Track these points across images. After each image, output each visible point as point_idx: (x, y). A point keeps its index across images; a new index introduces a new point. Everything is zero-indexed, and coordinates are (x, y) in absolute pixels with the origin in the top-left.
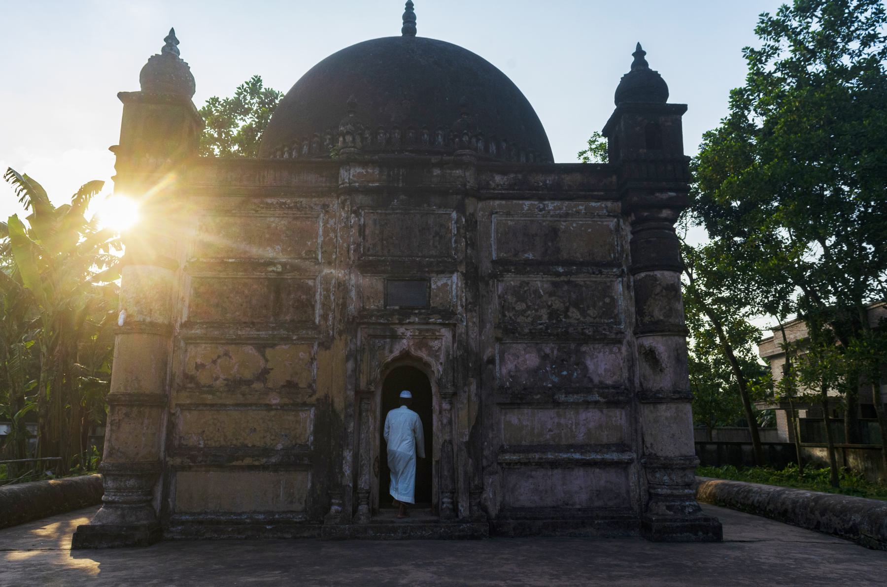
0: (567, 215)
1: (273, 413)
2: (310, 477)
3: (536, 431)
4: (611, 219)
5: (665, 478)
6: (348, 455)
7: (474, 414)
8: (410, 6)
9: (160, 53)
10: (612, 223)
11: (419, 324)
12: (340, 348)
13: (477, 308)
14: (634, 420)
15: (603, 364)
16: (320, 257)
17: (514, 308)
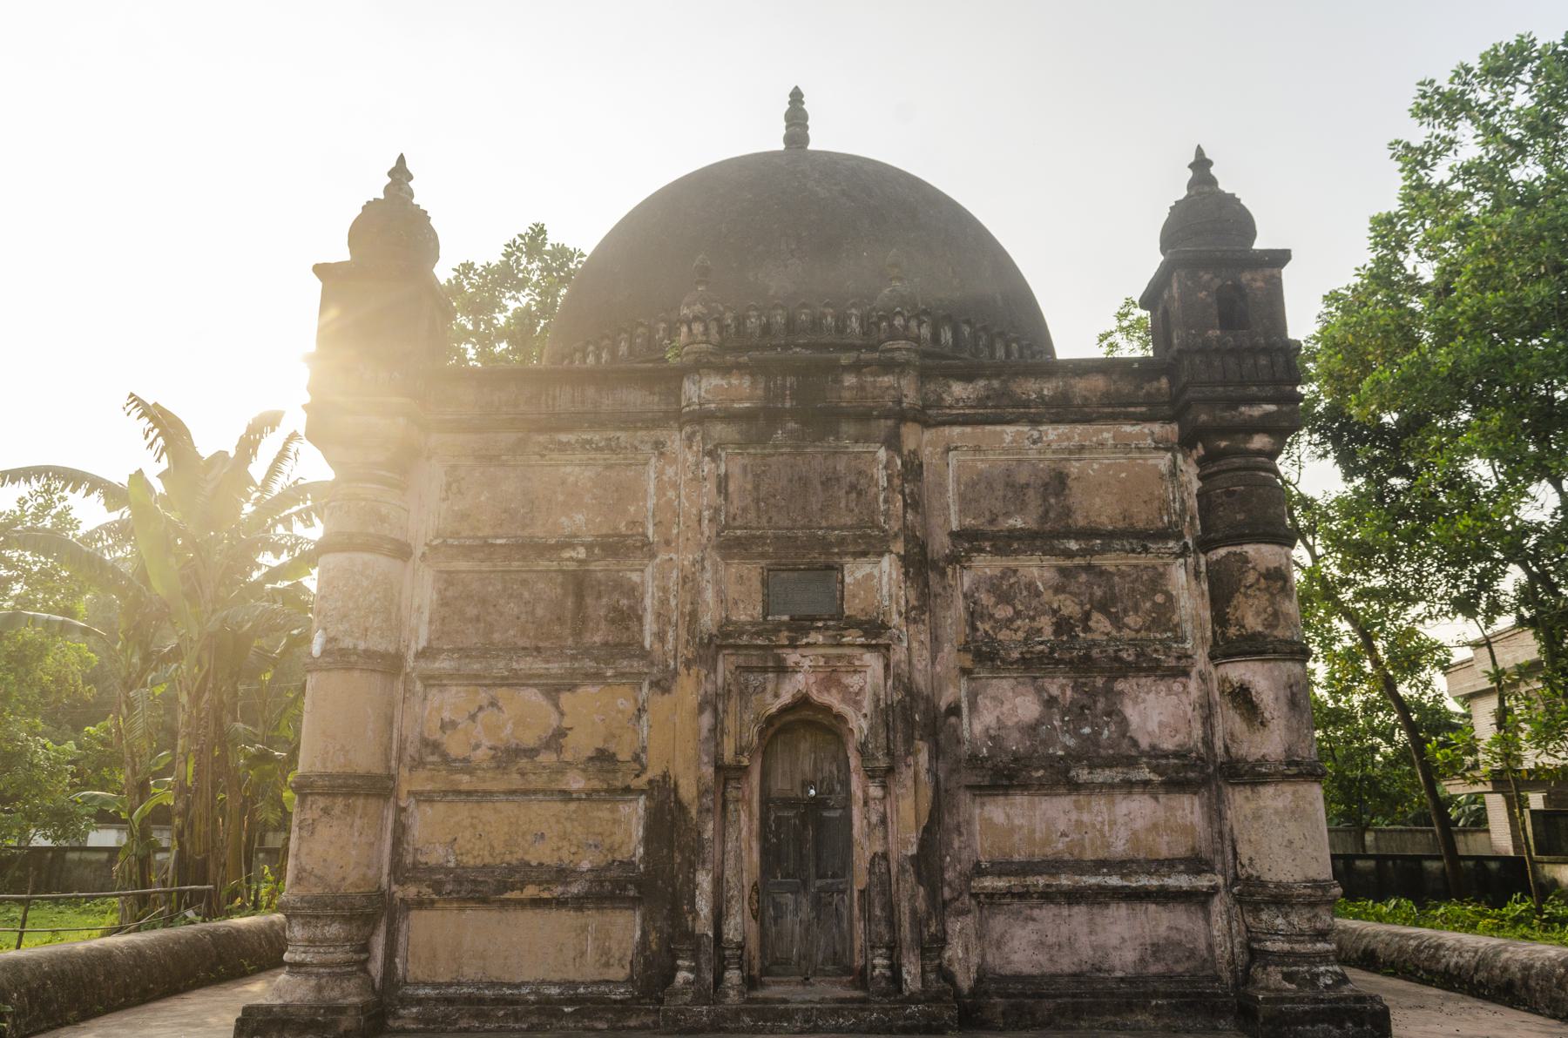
0: (1081, 448)
1: (573, 806)
2: (638, 920)
3: (1038, 835)
4: (1162, 454)
5: (1279, 921)
6: (704, 880)
7: (925, 805)
8: (796, 97)
9: (382, 196)
10: (1163, 461)
11: (824, 645)
12: (688, 691)
13: (926, 617)
14: (1216, 813)
15: (1156, 714)
16: (650, 532)
17: (991, 616)
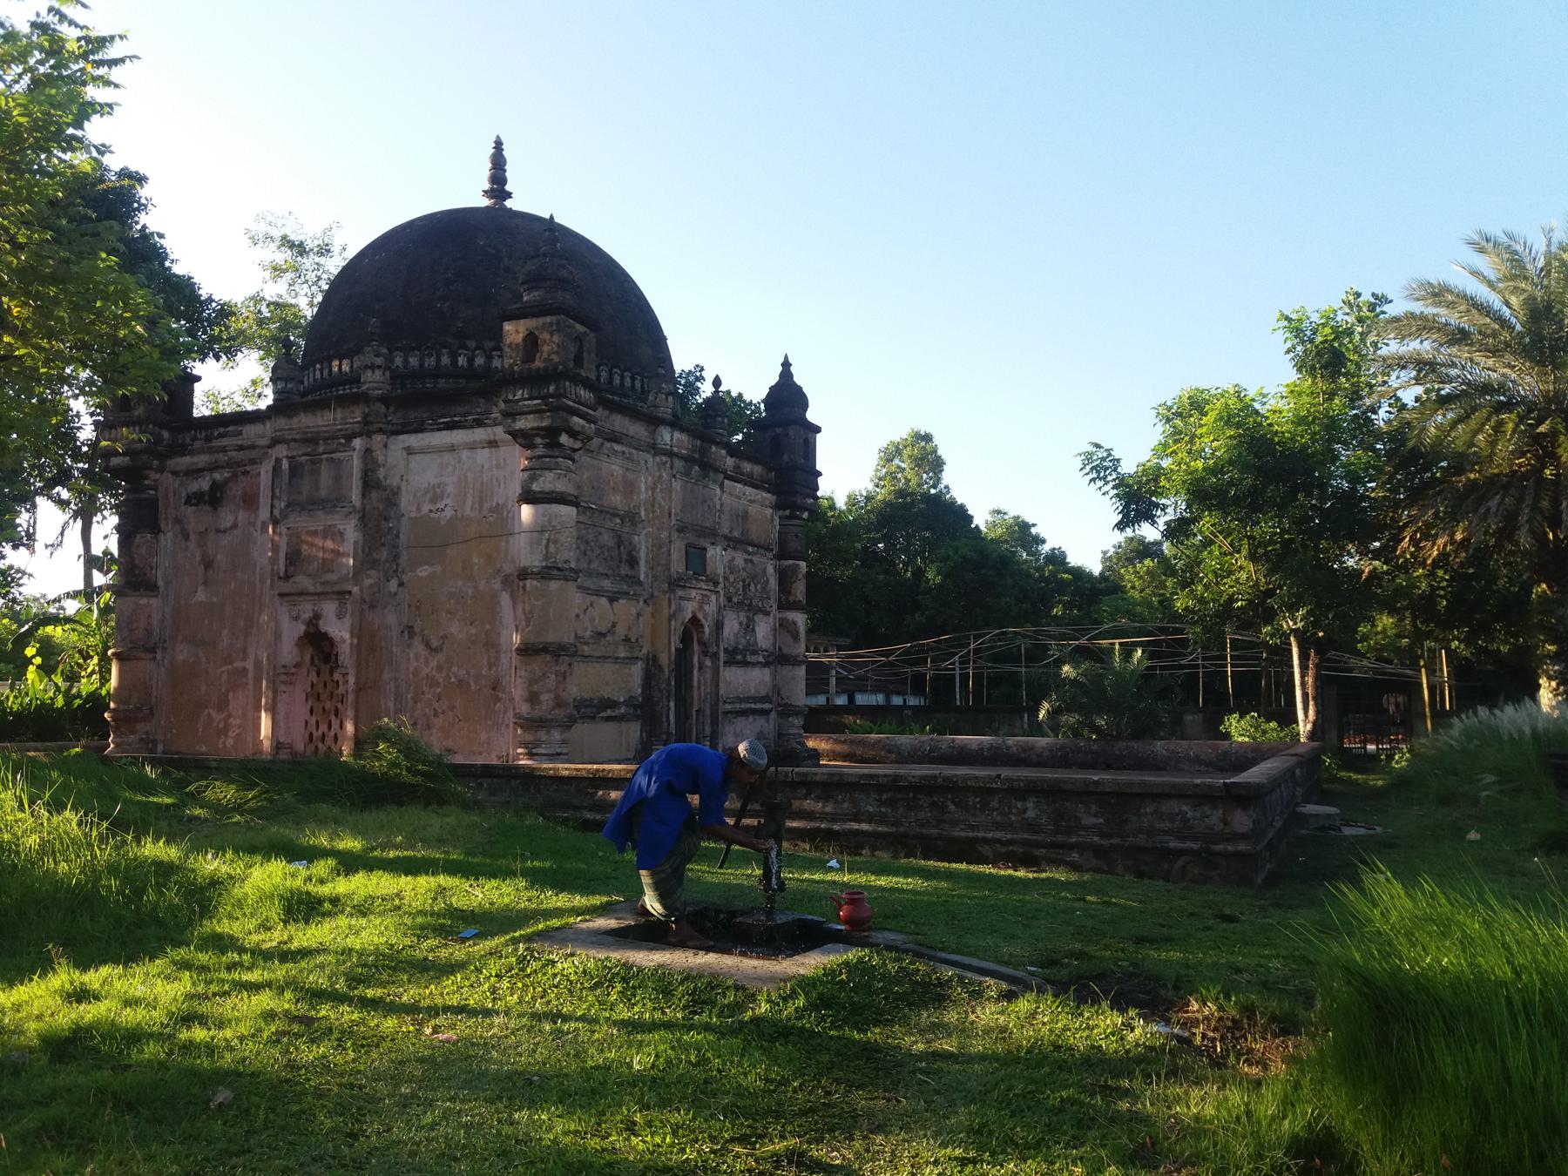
8: (498, 145)
10: (769, 512)
14: (774, 676)
